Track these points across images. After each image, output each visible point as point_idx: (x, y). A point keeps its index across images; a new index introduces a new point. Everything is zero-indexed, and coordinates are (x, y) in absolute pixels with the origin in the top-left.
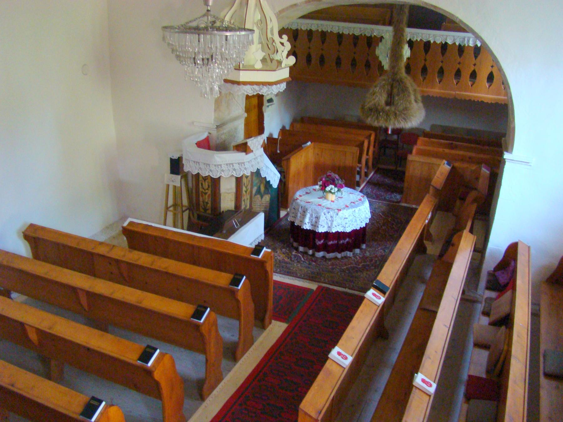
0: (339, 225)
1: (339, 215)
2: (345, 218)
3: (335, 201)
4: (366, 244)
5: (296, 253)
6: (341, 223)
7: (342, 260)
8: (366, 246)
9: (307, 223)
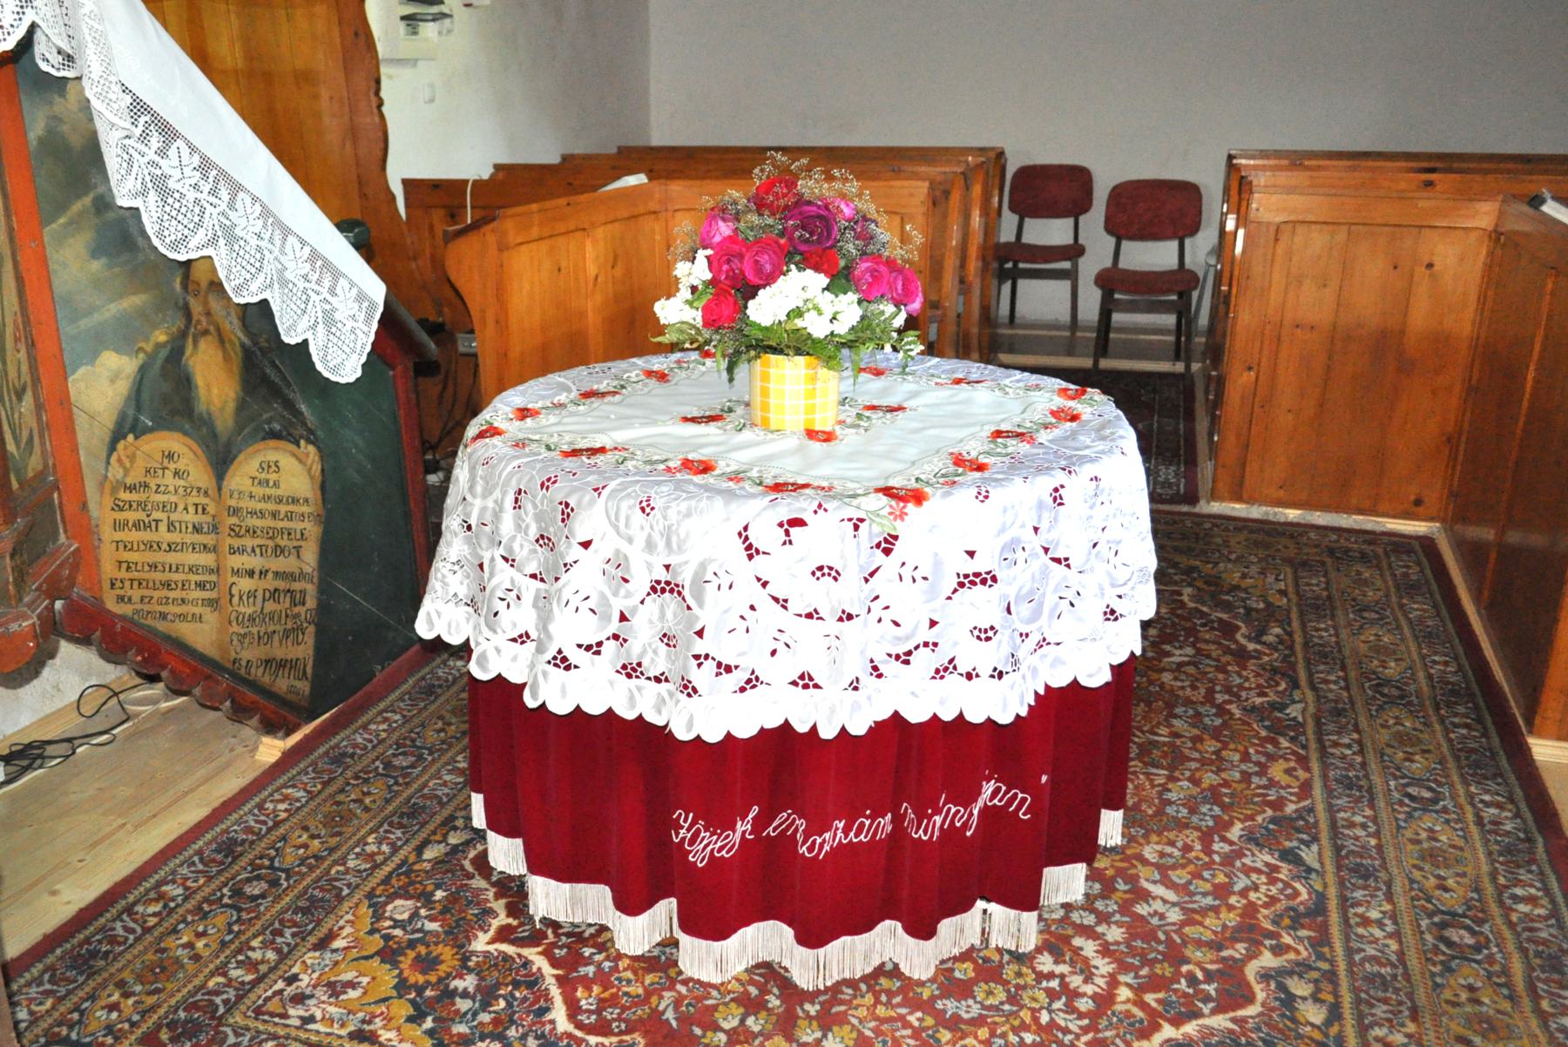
0: (905, 658)
1: (898, 547)
2: (967, 581)
3: (838, 430)
4: (1127, 809)
5: (504, 935)
6: (930, 636)
7: (949, 1006)
8: (1128, 824)
9: (574, 656)
